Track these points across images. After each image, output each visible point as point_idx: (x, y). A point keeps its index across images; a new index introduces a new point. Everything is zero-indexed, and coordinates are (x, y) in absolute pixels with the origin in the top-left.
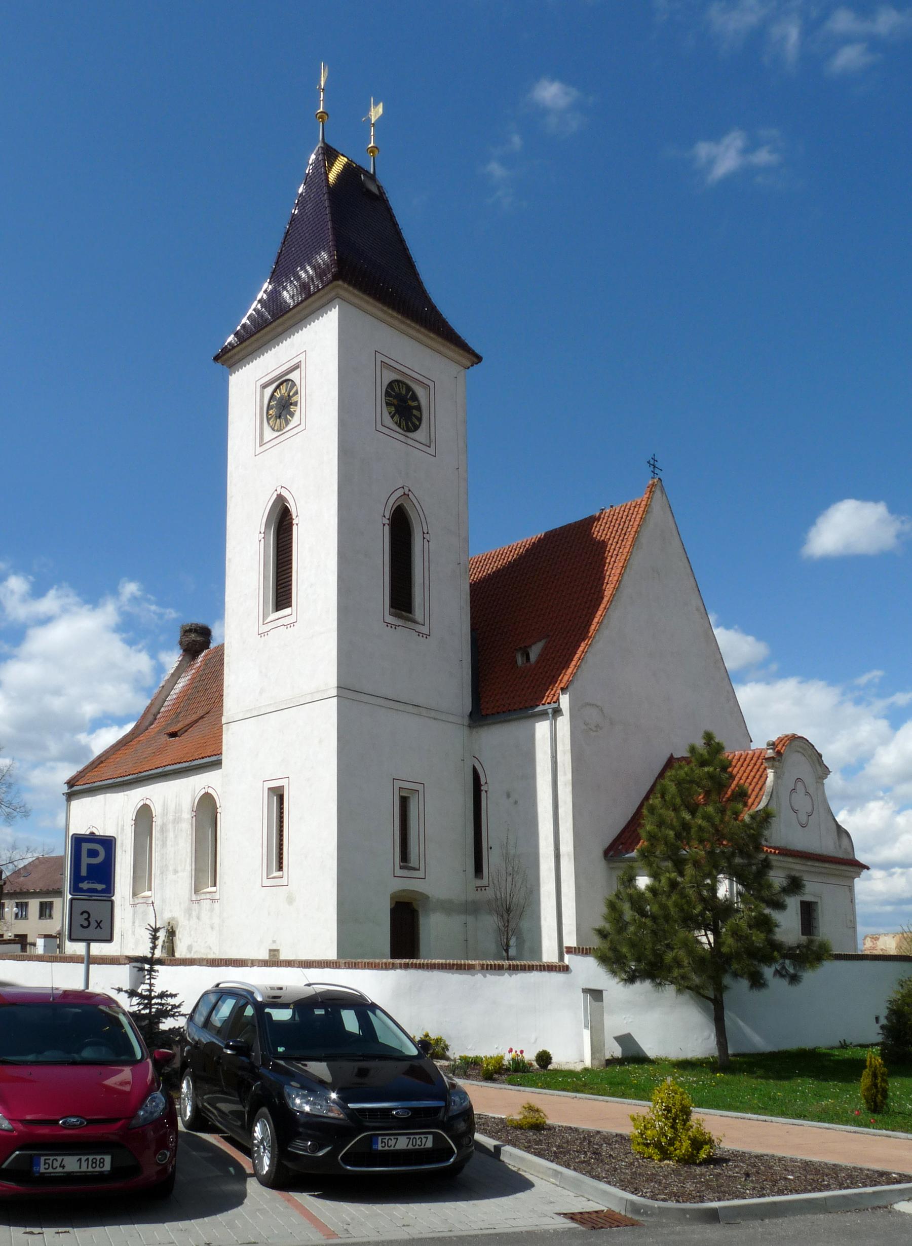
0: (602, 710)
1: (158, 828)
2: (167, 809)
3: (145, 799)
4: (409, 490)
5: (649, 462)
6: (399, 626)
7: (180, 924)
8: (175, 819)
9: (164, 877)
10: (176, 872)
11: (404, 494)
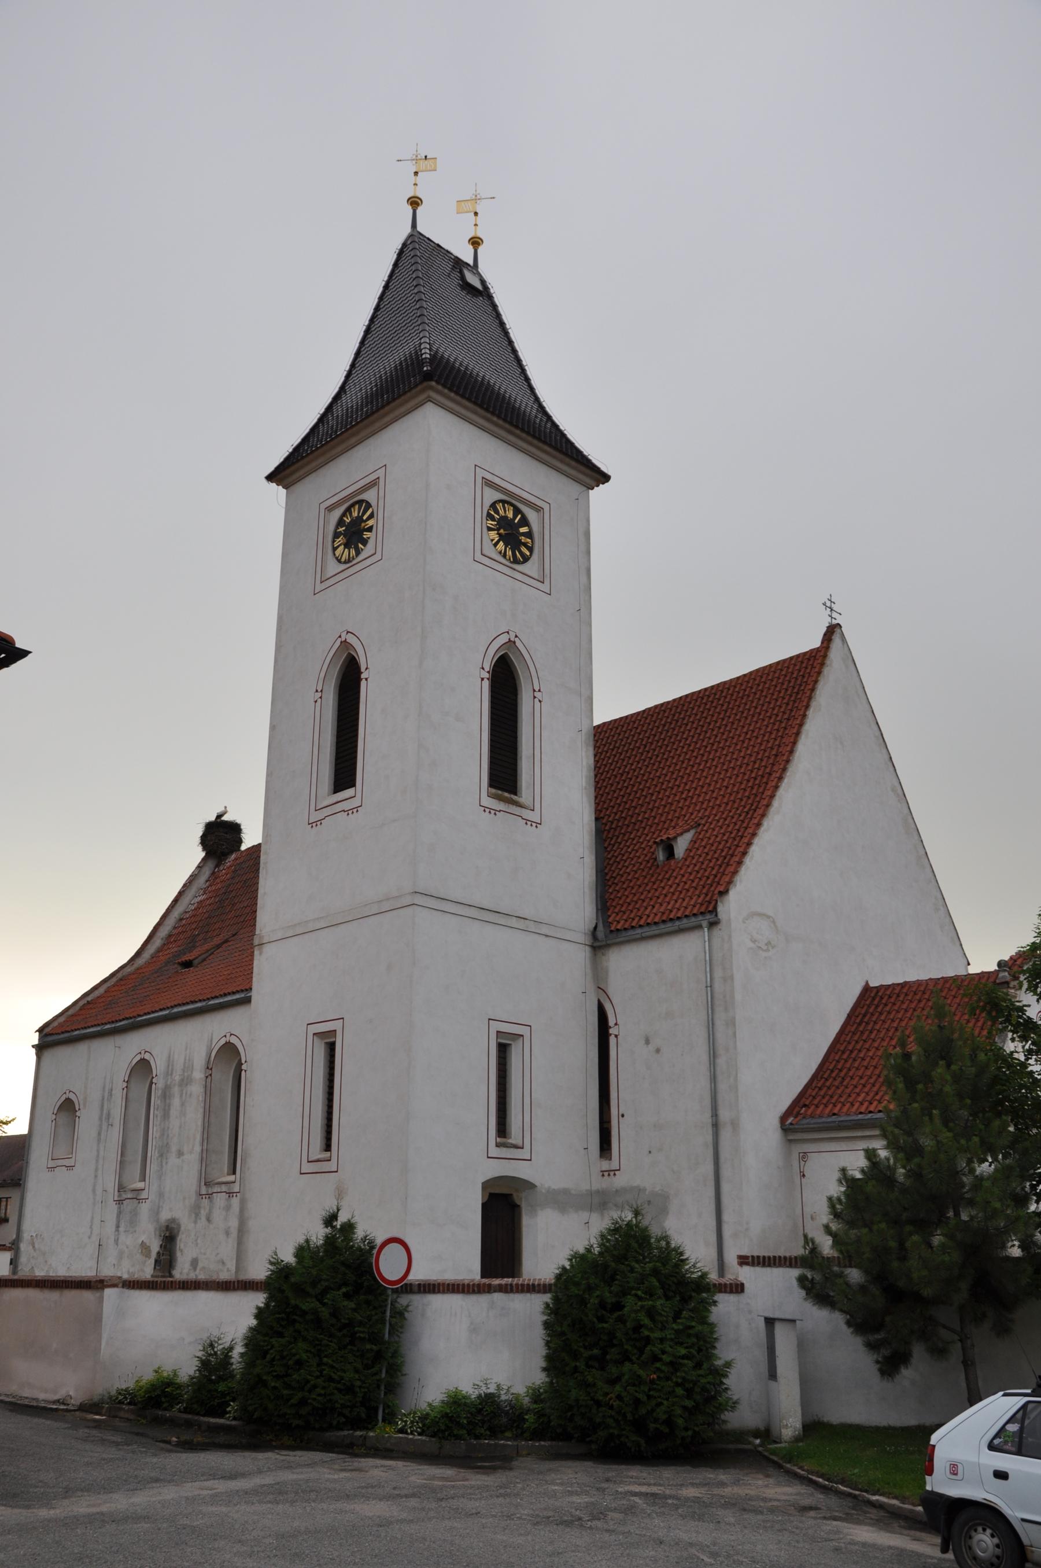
0: (774, 922)
2: (173, 1065)
3: (143, 1052)
4: (516, 636)
5: (824, 604)
6: (500, 811)
7: (182, 1228)
8: (182, 1080)
11: (510, 641)
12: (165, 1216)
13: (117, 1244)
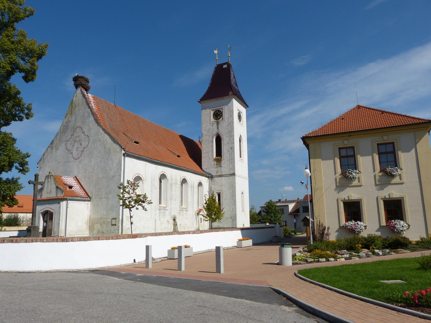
1: (170, 184)
3: (163, 172)
7: (177, 217)
9: (172, 201)
10: (175, 200)
12: (173, 214)
13: (160, 220)
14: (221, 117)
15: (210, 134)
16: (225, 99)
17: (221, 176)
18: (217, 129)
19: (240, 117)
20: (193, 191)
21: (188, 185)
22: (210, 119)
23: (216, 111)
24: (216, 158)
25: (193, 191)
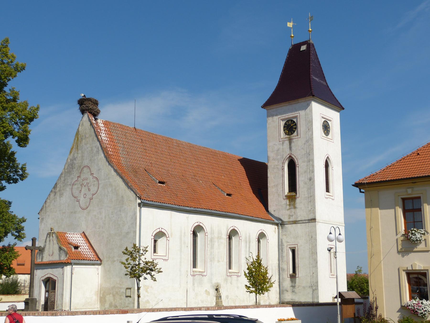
7: (222, 286)
10: (219, 261)
14: (295, 131)
15: (279, 157)
16: (302, 102)
17: (295, 222)
18: (289, 150)
19: (326, 128)
20: (249, 247)
21: (240, 238)
22: (280, 135)
23: (288, 121)
24: (288, 195)
25: (249, 247)
